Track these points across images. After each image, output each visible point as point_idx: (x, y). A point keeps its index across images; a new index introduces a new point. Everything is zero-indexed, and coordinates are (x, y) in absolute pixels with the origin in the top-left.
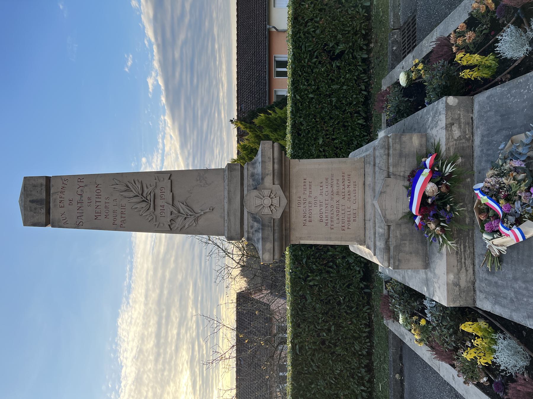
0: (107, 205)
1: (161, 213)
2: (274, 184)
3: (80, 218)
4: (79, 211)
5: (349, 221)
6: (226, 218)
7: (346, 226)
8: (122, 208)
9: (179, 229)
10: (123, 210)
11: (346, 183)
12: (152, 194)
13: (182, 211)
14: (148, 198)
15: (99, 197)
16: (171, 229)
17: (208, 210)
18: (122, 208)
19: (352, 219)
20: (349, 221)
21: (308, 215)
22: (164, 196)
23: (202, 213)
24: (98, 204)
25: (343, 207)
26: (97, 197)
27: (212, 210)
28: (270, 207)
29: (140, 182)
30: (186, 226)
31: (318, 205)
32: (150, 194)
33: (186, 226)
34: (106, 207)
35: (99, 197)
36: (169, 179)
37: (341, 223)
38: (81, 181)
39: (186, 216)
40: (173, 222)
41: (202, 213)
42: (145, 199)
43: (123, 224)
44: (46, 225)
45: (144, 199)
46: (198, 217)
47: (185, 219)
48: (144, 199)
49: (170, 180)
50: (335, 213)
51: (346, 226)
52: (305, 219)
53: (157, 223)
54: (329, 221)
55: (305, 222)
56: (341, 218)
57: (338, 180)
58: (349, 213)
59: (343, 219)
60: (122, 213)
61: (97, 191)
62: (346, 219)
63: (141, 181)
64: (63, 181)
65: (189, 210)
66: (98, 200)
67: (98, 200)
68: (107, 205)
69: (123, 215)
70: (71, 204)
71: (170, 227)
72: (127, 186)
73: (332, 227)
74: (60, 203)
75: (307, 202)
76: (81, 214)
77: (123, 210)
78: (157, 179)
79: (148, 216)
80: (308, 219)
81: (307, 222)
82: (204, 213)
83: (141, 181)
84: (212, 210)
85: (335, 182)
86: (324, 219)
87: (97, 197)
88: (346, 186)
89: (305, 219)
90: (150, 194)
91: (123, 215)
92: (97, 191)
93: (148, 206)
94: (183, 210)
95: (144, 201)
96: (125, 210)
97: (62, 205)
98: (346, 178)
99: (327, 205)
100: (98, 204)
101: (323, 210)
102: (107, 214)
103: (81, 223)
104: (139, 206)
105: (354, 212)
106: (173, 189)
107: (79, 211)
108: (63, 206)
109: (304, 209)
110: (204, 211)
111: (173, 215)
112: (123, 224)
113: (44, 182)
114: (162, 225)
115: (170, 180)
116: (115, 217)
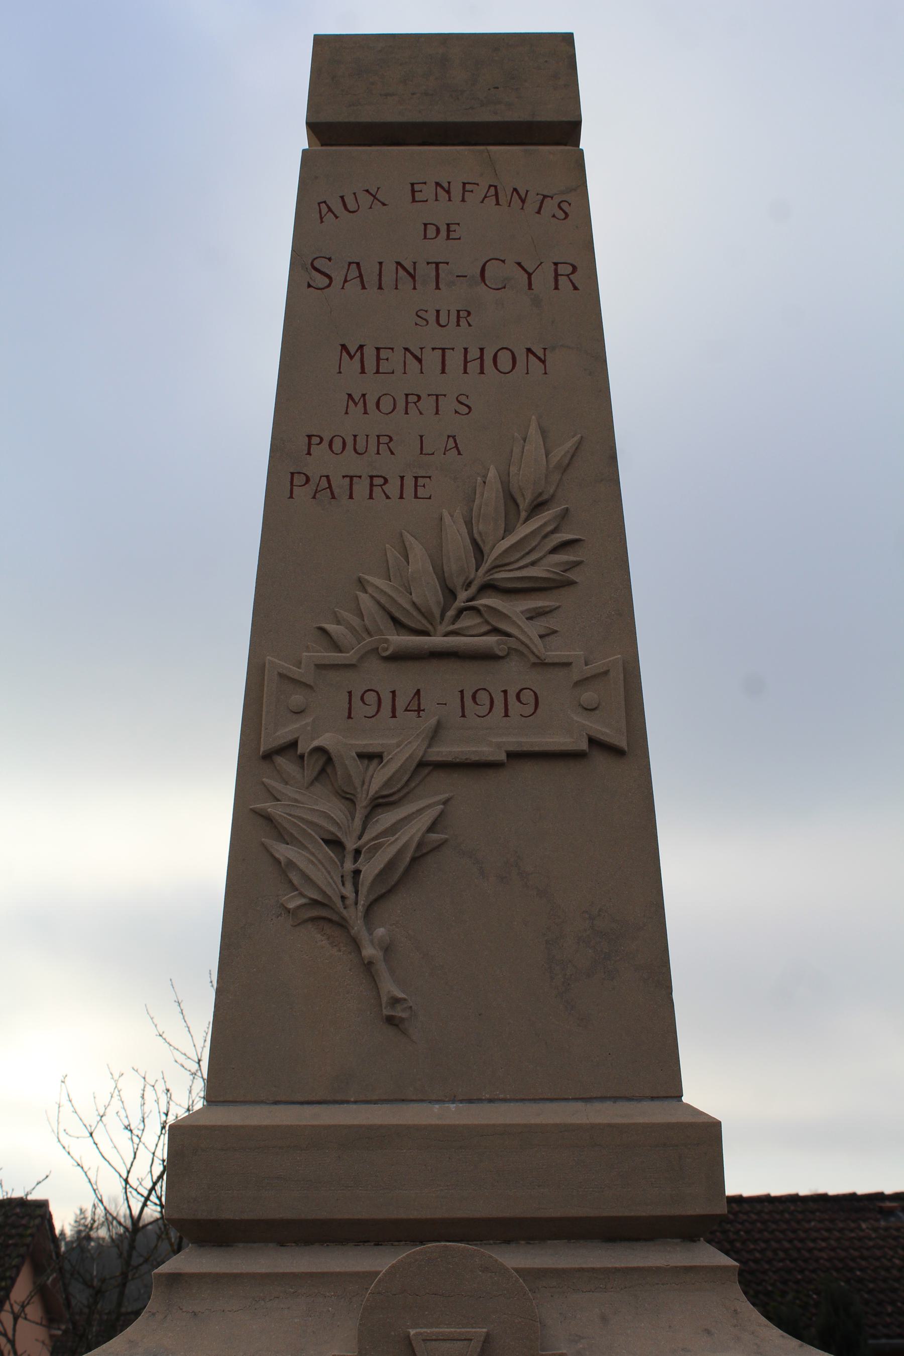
0: (427, 404)
1: (371, 698)
3: (354, 272)
4: (389, 269)
8: (409, 483)
9: (270, 807)
10: (393, 488)
13: (387, 819)
14: (467, 621)
15: (474, 366)
16: (268, 757)
17: (389, 987)
18: (409, 483)
23: (369, 951)
24: (432, 360)
26: (474, 353)
27: (391, 1021)
29: (571, 575)
30: (284, 851)
32: (496, 631)
33: (284, 851)
34: (412, 399)
35: (474, 366)
36: (593, 742)
38: (563, 281)
39: (351, 845)
40: (313, 767)
41: (369, 951)
42: (459, 603)
43: (310, 489)
44: (314, 128)
45: (463, 596)
46: (342, 925)
47: (335, 843)
48: (463, 596)
49: (584, 746)
60: (377, 482)
61: (505, 360)
63: (571, 583)
64: (557, 199)
65: (390, 865)
66: (455, 360)
67: (455, 360)
68: (427, 404)
69: (361, 488)
72: (538, 506)
74: (437, 184)
76: (371, 277)
77: (393, 488)
78: (590, 670)
79: (355, 621)
82: (368, 966)
83: (571, 583)
84: (391, 1021)
87: (474, 353)
91: (361, 488)
92: (505, 360)
93: (421, 622)
94: (392, 830)
95: (451, 594)
97: (428, 192)
100: (432, 360)
102: (371, 405)
103: (322, 281)
104: (419, 560)
106: (528, 771)
107: (389, 269)
108: (418, 196)
110: (381, 967)
111: (355, 767)
112: (310, 489)
113: (547, 114)
114: (297, 699)
115: (584, 746)
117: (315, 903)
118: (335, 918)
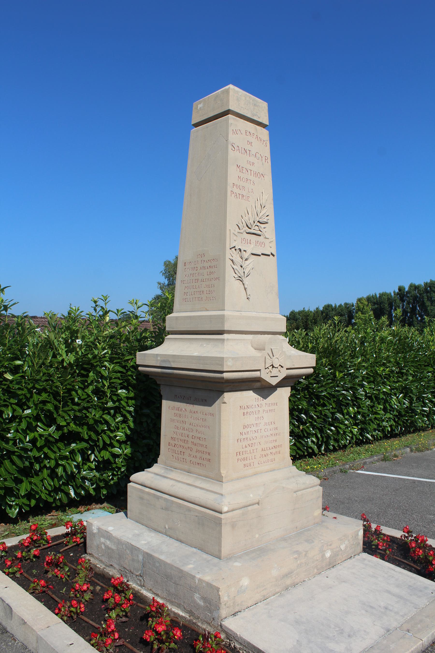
2: (287, 369)
5: (244, 459)
6: (244, 314)
7: (240, 457)
11: (274, 451)
12: (259, 232)
19: (246, 462)
20: (244, 459)
21: (249, 410)
22: (258, 245)
25: (255, 451)
28: (272, 365)
31: (258, 422)
36: (272, 254)
37: (243, 450)
50: (250, 442)
51: (240, 457)
52: (246, 407)
53: (236, 233)
54: (244, 436)
55: (243, 407)
56: (246, 449)
57: (276, 441)
58: (251, 458)
59: (246, 452)
62: (245, 456)
70: (249, 144)
71: (233, 248)
73: (239, 440)
75: (259, 409)
80: (245, 411)
81: (243, 411)
85: (274, 438)
86: (246, 430)
88: (271, 451)
89: (246, 407)
90: (260, 230)
96: (245, 199)
98: (277, 450)
99: (257, 432)
101: (254, 429)
105: (252, 464)
109: (254, 406)
116: (238, 187)
117: (240, 277)
118: (241, 280)
